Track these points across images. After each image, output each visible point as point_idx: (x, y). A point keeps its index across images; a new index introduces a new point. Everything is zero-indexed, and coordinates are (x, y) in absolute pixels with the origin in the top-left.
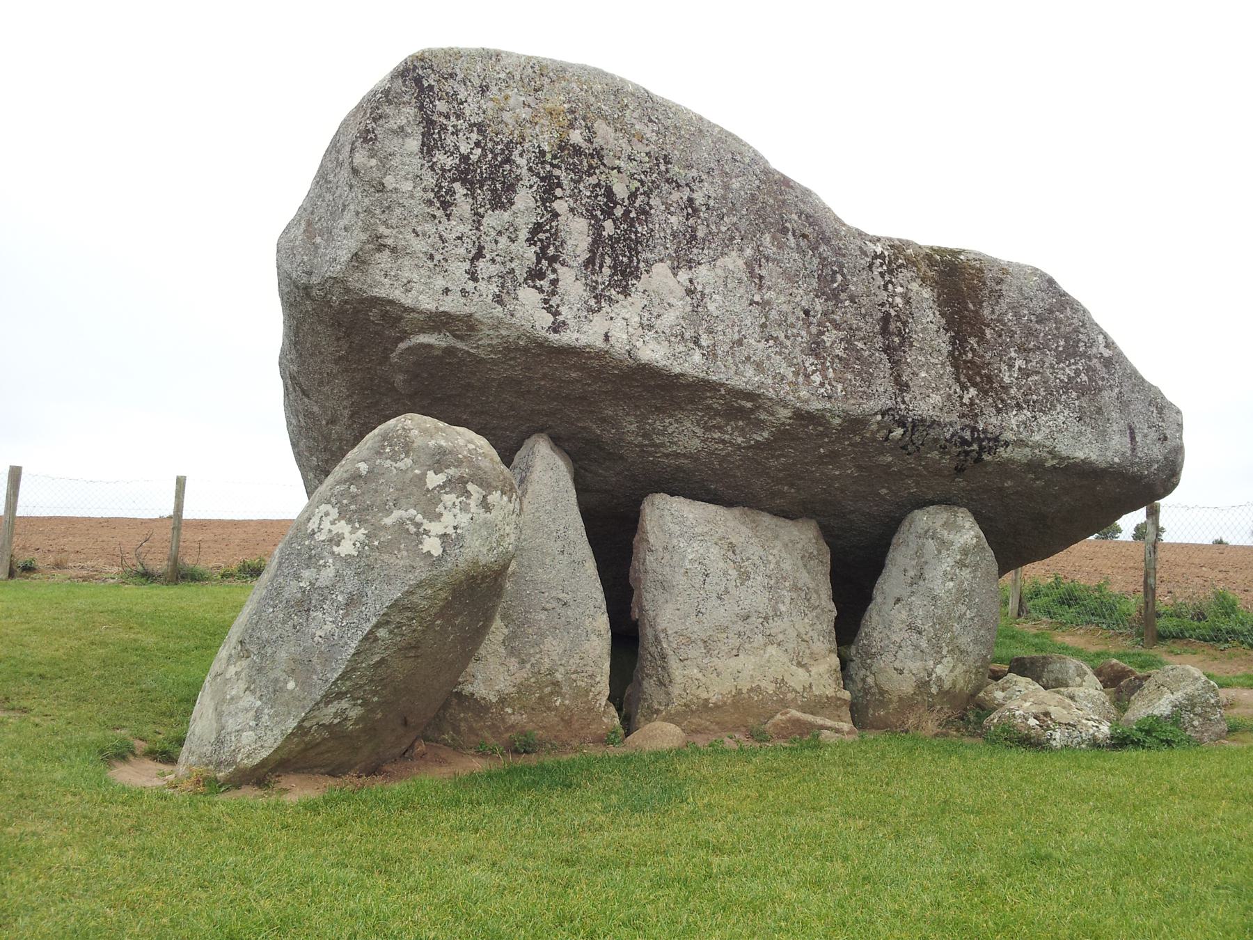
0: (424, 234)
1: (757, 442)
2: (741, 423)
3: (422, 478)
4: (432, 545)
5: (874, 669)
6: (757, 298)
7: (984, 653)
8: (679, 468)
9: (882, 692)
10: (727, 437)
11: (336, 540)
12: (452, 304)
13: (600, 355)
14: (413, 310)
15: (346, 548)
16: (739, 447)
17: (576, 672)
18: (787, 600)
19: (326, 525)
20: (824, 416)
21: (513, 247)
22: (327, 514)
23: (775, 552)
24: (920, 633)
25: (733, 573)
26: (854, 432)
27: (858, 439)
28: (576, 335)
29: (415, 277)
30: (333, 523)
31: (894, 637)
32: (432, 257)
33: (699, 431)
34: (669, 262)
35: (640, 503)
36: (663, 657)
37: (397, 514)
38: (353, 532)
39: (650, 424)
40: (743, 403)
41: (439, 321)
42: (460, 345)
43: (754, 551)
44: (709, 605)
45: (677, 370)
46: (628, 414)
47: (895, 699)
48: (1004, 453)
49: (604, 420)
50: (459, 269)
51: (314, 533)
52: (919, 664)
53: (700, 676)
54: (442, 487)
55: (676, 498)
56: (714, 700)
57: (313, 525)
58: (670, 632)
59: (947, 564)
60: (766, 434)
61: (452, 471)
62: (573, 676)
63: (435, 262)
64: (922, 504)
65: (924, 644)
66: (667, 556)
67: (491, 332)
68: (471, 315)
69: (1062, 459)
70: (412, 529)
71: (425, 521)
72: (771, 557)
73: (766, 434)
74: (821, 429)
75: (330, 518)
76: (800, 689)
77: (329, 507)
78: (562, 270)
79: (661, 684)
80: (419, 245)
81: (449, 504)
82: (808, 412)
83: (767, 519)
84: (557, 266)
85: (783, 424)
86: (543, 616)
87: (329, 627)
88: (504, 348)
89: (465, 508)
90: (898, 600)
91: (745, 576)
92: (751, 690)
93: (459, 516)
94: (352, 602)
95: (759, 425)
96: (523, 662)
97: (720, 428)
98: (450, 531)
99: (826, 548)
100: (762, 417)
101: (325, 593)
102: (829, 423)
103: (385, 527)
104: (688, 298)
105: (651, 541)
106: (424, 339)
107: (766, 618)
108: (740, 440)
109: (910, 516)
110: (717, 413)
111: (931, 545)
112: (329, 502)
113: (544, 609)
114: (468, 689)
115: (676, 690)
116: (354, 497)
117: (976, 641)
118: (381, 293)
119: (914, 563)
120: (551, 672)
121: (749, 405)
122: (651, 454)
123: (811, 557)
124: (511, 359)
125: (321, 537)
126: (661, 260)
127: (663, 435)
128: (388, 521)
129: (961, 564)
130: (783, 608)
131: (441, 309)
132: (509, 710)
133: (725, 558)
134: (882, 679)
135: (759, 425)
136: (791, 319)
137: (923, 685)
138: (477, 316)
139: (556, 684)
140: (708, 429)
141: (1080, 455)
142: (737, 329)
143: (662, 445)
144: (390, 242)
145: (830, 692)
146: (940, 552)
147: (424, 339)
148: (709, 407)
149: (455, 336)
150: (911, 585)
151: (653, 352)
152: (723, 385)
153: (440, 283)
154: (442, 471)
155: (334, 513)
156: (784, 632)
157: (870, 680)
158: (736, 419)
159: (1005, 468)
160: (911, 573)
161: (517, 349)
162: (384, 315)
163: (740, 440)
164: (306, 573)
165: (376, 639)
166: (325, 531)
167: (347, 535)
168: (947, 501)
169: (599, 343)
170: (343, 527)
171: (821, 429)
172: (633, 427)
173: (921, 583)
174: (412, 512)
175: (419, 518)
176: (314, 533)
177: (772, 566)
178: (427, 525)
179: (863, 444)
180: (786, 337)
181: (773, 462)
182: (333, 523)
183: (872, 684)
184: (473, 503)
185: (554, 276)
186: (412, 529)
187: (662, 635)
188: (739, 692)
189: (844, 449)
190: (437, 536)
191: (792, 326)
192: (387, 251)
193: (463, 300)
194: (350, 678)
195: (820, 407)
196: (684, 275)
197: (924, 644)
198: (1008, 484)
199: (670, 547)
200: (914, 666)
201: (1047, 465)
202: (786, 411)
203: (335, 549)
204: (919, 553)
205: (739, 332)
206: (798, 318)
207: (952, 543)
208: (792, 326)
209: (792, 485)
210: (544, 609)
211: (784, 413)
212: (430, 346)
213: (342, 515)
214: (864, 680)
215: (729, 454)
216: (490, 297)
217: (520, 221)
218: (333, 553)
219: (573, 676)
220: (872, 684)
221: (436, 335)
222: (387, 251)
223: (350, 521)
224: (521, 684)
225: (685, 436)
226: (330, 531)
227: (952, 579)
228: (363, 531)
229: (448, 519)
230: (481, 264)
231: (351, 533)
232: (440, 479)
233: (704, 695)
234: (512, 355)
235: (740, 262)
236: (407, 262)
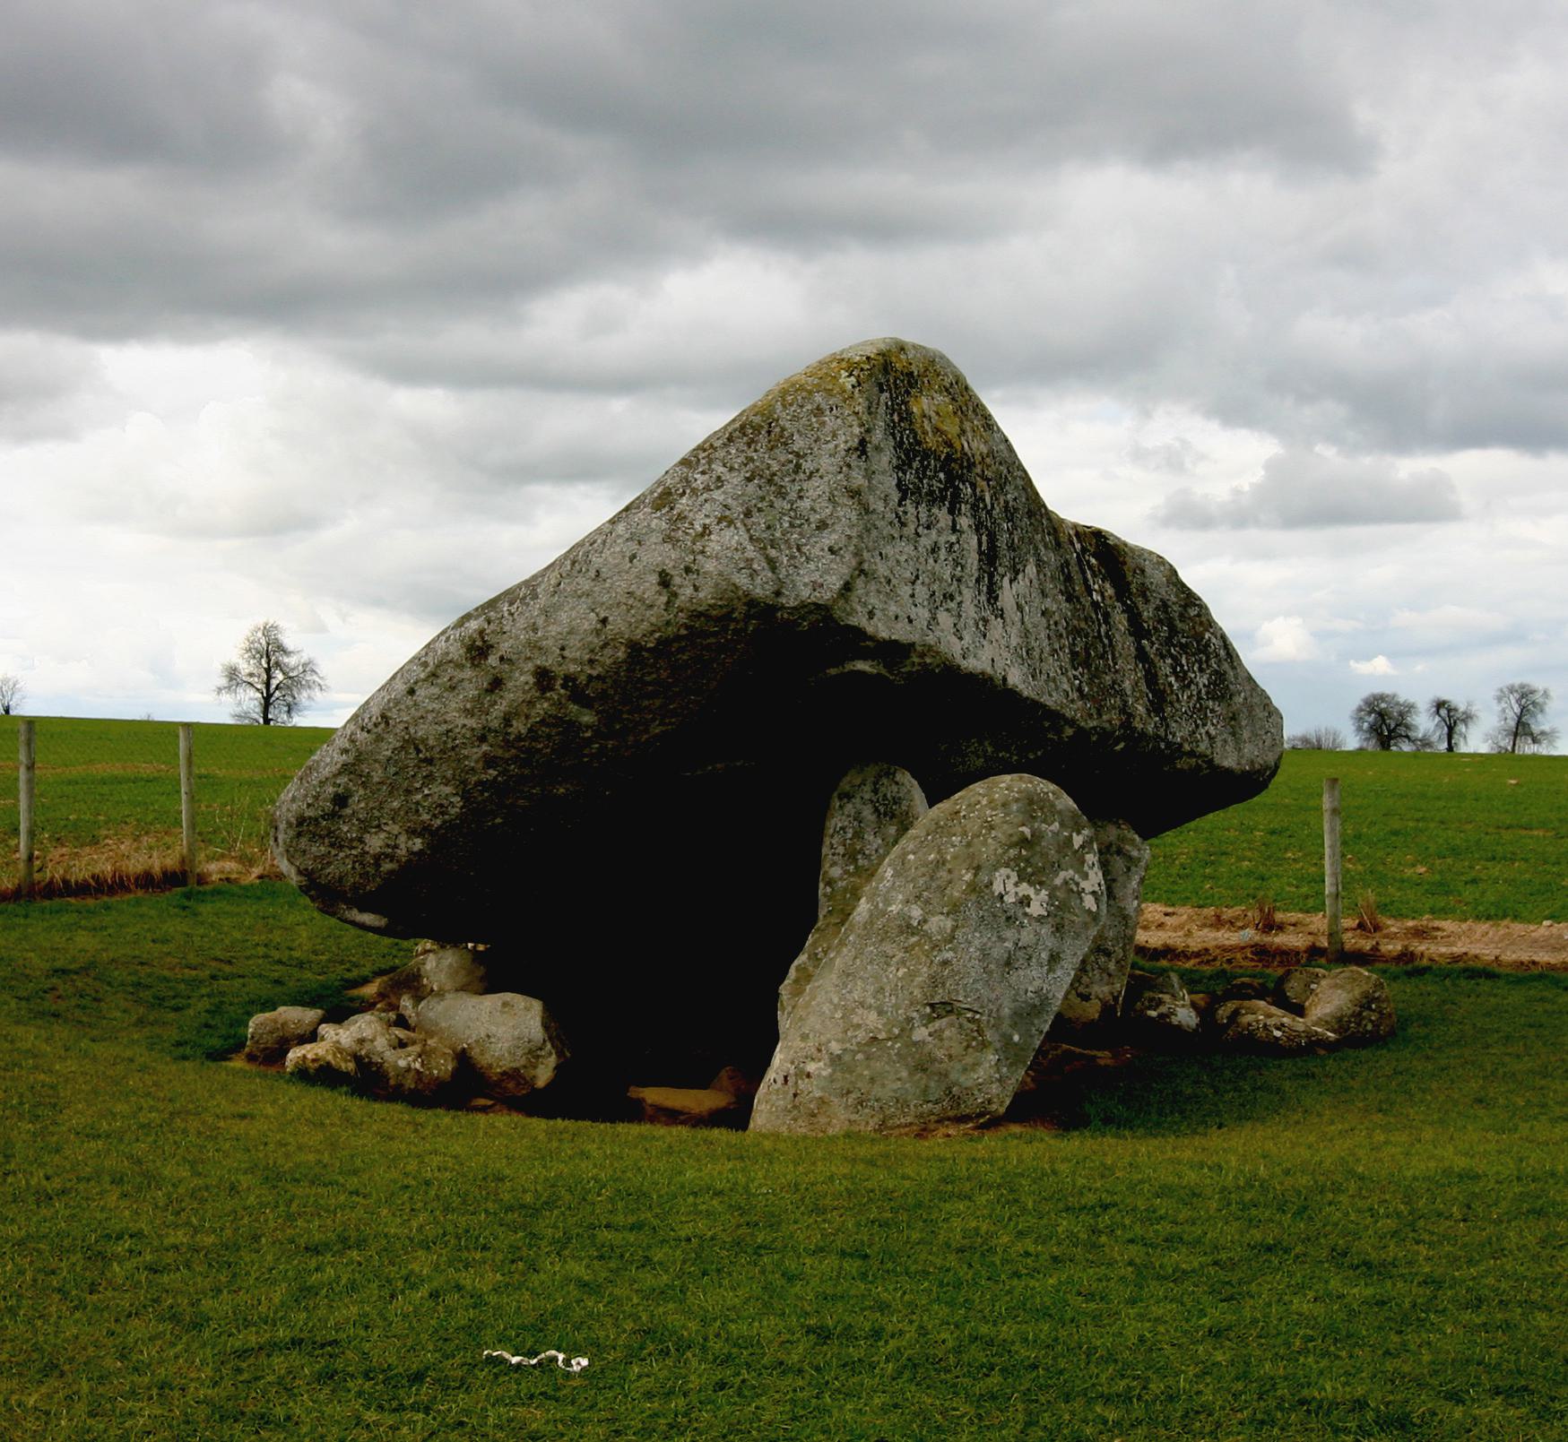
4: (1089, 902)
11: (1025, 901)
12: (901, 633)
14: (872, 638)
15: (1036, 909)
19: (1010, 887)
21: (937, 567)
30: (1016, 885)
32: (889, 582)
37: (1062, 874)
38: (1037, 892)
41: (894, 651)
42: (884, 672)
50: (905, 590)
51: (1001, 897)
52: (1106, 989)
57: (998, 888)
61: (1086, 832)
65: (1112, 966)
77: (1008, 871)
78: (965, 591)
80: (882, 570)
87: (1037, 983)
94: (1054, 958)
101: (1027, 952)
106: (862, 666)
112: (1007, 866)
116: (1027, 861)
118: (853, 621)
125: (1010, 899)
128: (1058, 881)
141: (1226, 764)
144: (866, 566)
147: (862, 666)
151: (1016, 678)
155: (1014, 877)
164: (1009, 934)
170: (1025, 889)
176: (1001, 897)
178: (1083, 884)
182: (1016, 885)
197: (1112, 966)
207: (1139, 860)
211: (1069, 732)
213: (1021, 879)
217: (942, 540)
218: (1026, 914)
223: (1030, 883)
229: (1091, 873)
230: (918, 587)
236: (873, 587)
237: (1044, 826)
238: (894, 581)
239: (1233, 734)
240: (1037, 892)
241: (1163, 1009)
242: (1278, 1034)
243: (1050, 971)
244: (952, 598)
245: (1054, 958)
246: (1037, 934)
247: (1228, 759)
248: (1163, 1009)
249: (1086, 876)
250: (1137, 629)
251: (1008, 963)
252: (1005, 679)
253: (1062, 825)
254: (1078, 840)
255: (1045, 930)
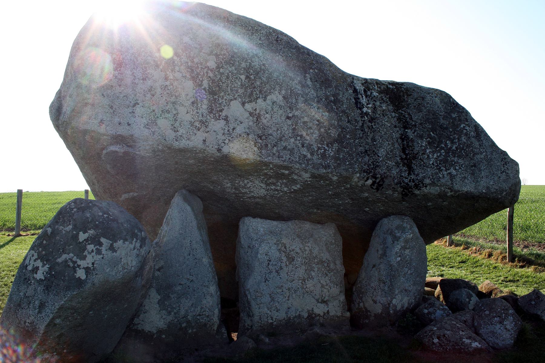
0: (108, 96)
1: (294, 190)
2: (285, 181)
3: (76, 236)
5: (364, 299)
6: (290, 115)
7: (419, 289)
8: (257, 203)
9: (367, 311)
10: (278, 188)
13: (203, 151)
14: (104, 135)
15: (40, 276)
16: (286, 193)
17: (199, 315)
18: (316, 269)
19: (32, 262)
20: (328, 176)
22: (33, 256)
23: (309, 245)
24: (384, 283)
25: (284, 259)
26: (346, 183)
27: (348, 186)
28: (188, 142)
29: (105, 118)
30: (35, 261)
31: (372, 285)
33: (263, 186)
34: (240, 100)
35: (239, 221)
36: (249, 303)
37: (64, 256)
38: (44, 265)
39: (237, 183)
40: (283, 171)
43: (296, 246)
44: (271, 276)
45: (245, 156)
46: (225, 179)
47: (373, 315)
48: (426, 190)
49: (213, 182)
52: (384, 299)
53: (268, 312)
54: (86, 240)
55: (256, 220)
56: (275, 323)
58: (251, 291)
59: (397, 248)
60: (298, 186)
61: (91, 232)
62: (198, 317)
63: (114, 109)
64: (387, 215)
66: (250, 251)
67: (145, 143)
68: (132, 136)
69: (456, 191)
70: (71, 265)
71: (78, 260)
72: (306, 248)
73: (298, 186)
74: (328, 182)
75: (34, 258)
76: (322, 314)
79: (249, 316)
81: (90, 250)
82: (319, 175)
83: (307, 226)
84: (177, 107)
85: (307, 181)
86: (179, 288)
87: (32, 318)
88: (153, 151)
89: (99, 252)
90: (374, 266)
91: (291, 259)
92: (296, 317)
93: (95, 257)
94: (42, 306)
95: (294, 182)
96: (169, 313)
97: (274, 184)
98: (90, 265)
99: (340, 238)
100: (295, 178)
102: (331, 179)
103: (58, 264)
104: (251, 118)
105: (242, 243)
106: (113, 148)
107: (304, 280)
108: (286, 189)
109: (381, 221)
110: (271, 177)
111: (390, 239)
113: (180, 284)
114: (140, 328)
115: (256, 318)
117: (414, 284)
119: (382, 247)
120: (185, 316)
121: (287, 172)
122: (241, 197)
123: (331, 244)
124: (157, 155)
126: (235, 99)
127: (245, 188)
128: (59, 260)
129: (404, 248)
130: (313, 274)
131: (118, 133)
132: (164, 336)
133: (279, 250)
134: (367, 305)
135: (294, 182)
136: (310, 125)
137: (386, 308)
138: (136, 135)
139: (188, 322)
140: (267, 185)
141: (465, 189)
142: (279, 132)
143: (246, 193)
144: (90, 101)
145: (339, 314)
146: (394, 242)
148: (266, 174)
149: (128, 146)
150: (380, 258)
152: (271, 163)
153: (117, 120)
154: (87, 232)
155: (36, 256)
156: (314, 286)
157: (361, 304)
158: (281, 179)
159: (426, 197)
160: (380, 252)
161: (159, 150)
162: (92, 138)
163: (286, 189)
165: (55, 325)
166: (31, 265)
167: (40, 268)
168: (400, 214)
169: (200, 146)
170: (39, 263)
171: (328, 182)
172: (229, 185)
173: (385, 258)
174: (71, 255)
175: (75, 259)
177: (307, 252)
178: (80, 262)
179: (351, 188)
180: (307, 134)
181: (305, 199)
182: (35, 261)
183: (363, 307)
184: (103, 249)
185: (175, 112)
186: (71, 265)
187: (247, 292)
188: (290, 319)
189: (341, 191)
190: (84, 268)
191: (311, 128)
192: (90, 106)
193: (128, 128)
194: (45, 344)
195: (324, 171)
196: (247, 106)
197: (386, 288)
198: (430, 204)
199: (251, 246)
200: (382, 299)
201: (448, 195)
202: (307, 174)
203: (35, 275)
204: (384, 242)
205: (281, 133)
206: (313, 124)
207: (400, 238)
208: (311, 128)
209: (318, 209)
210: (180, 284)
212: (117, 152)
214: (359, 304)
215: (281, 196)
216: (143, 125)
218: (34, 277)
219: (198, 317)
220: (363, 307)
221: (118, 146)
222: (90, 106)
224: (169, 322)
225: (256, 188)
226: (34, 265)
227: (400, 256)
228: (47, 266)
231: (43, 267)
232: (86, 236)
233: (270, 321)
234: (157, 154)
235: (280, 97)
237: (62, 227)
238: (114, 107)
239: (473, 174)
240: (44, 265)
241: (431, 310)
242: (436, 341)
243: (40, 312)
244: (168, 112)
245: (42, 306)
246: (35, 290)
247: (468, 187)
248: (431, 310)
249: (84, 258)
250: (405, 124)
251: (19, 305)
252: (219, 150)
253: (75, 227)
254: (82, 237)
255: (40, 289)
